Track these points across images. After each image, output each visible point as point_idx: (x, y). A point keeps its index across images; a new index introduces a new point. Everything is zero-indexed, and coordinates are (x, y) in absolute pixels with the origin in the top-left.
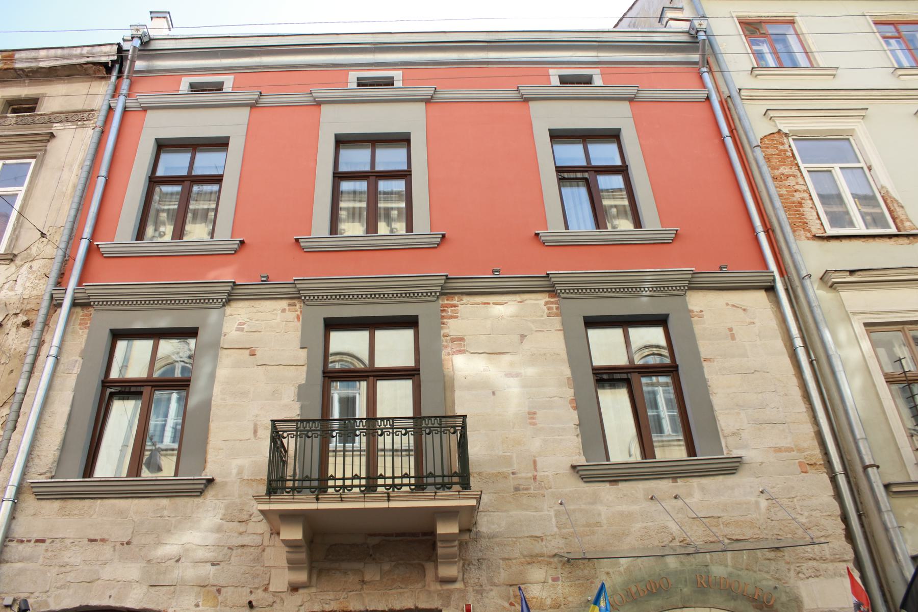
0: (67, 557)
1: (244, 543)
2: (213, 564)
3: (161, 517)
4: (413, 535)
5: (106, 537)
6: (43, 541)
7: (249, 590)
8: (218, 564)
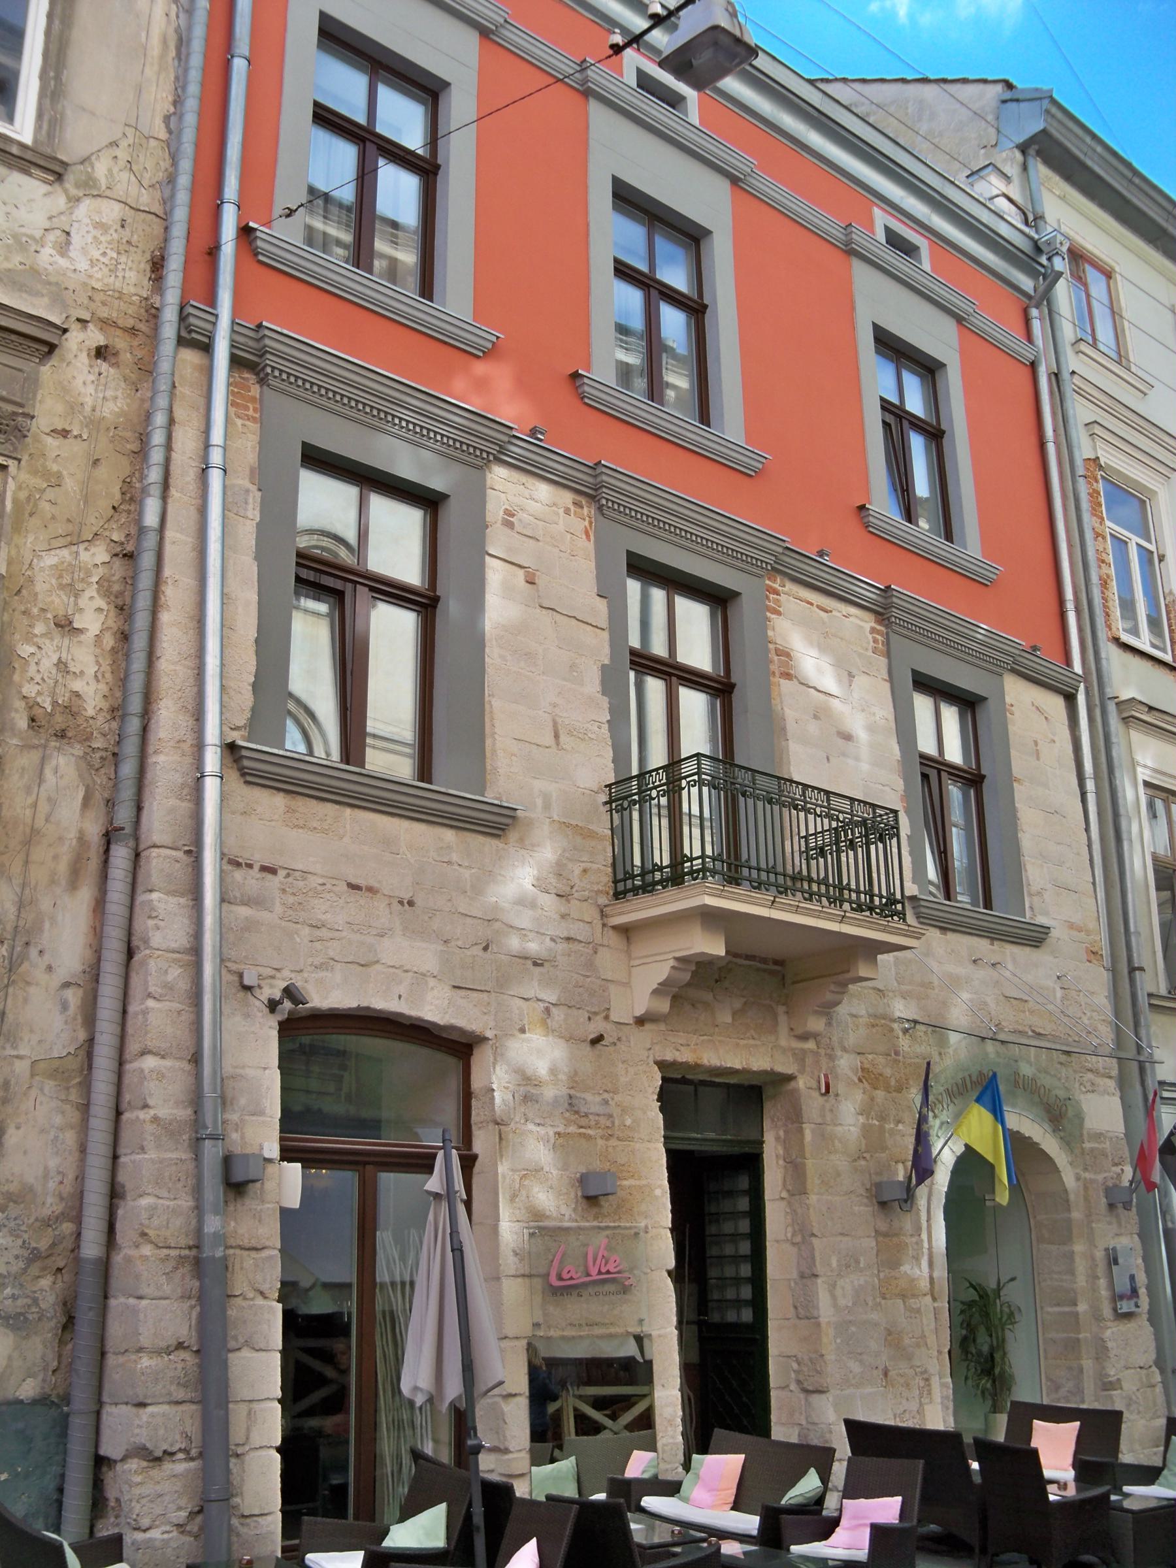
0: (320, 909)
2: (535, 964)
3: (449, 863)
4: (764, 960)
5: (376, 885)
6: (272, 871)
8: (542, 965)
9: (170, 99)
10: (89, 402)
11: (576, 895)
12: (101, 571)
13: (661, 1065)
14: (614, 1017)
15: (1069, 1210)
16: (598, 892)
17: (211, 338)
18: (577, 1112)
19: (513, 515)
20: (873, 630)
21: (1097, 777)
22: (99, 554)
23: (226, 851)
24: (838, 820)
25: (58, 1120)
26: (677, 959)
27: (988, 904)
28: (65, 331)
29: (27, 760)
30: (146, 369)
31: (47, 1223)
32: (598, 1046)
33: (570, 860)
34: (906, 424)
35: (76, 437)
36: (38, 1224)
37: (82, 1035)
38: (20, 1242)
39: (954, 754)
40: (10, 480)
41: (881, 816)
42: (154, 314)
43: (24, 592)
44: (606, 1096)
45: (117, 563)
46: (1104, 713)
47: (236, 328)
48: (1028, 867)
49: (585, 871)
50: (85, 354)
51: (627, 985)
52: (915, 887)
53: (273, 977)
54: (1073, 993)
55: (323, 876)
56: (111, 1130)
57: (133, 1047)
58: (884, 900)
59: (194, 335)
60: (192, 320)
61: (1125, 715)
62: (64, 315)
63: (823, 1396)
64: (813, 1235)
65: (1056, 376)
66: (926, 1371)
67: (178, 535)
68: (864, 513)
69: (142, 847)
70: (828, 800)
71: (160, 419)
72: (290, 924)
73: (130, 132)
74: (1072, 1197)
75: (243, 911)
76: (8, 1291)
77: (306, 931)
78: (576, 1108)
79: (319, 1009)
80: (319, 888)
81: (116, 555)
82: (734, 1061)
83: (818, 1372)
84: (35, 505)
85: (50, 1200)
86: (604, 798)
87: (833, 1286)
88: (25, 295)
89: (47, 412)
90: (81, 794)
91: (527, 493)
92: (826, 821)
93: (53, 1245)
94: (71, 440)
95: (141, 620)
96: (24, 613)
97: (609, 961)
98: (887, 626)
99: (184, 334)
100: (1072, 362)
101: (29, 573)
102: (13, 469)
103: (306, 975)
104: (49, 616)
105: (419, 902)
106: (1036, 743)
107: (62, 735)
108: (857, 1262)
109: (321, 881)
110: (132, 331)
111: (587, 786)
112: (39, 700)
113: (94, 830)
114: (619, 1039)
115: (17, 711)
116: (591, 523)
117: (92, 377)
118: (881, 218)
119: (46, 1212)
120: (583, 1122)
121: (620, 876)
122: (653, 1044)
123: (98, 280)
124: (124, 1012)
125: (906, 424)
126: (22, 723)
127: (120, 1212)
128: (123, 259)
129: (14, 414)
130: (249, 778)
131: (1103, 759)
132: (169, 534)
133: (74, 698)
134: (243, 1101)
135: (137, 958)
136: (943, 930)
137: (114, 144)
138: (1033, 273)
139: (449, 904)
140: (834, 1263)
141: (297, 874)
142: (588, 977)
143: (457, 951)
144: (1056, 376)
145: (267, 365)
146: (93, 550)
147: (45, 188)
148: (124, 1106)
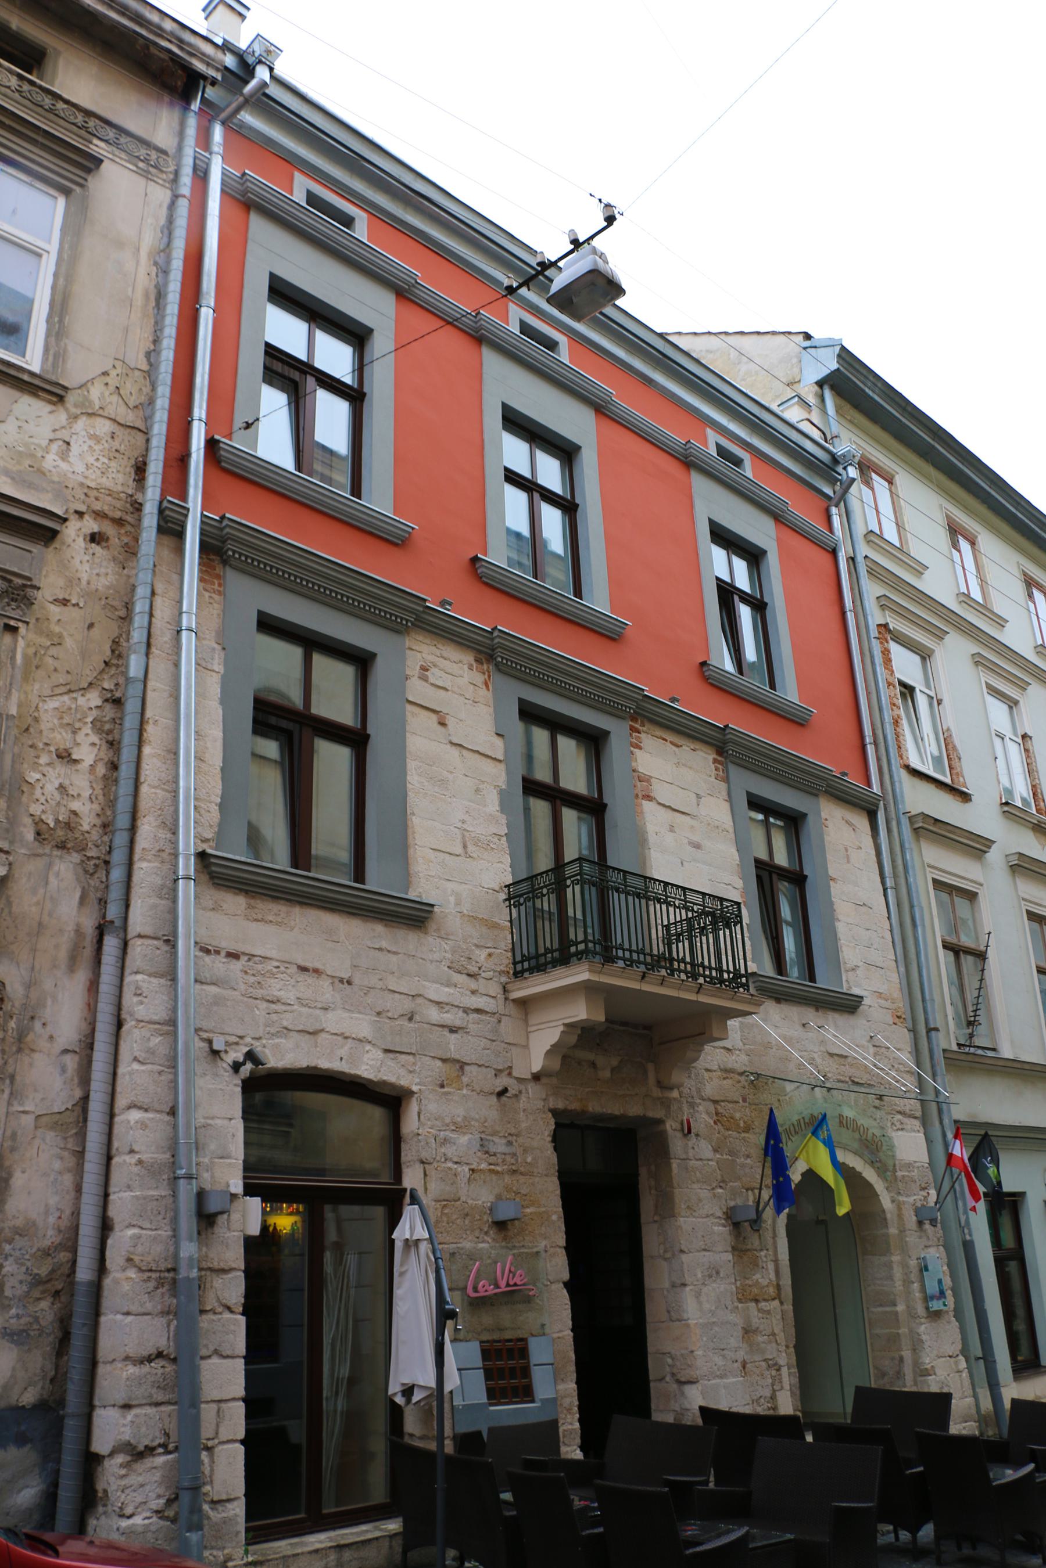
0: (275, 988)
1: (480, 1006)
3: (380, 949)
6: (233, 956)
7: (493, 1072)
9: (151, 339)
10: (85, 577)
11: (483, 974)
12: (95, 713)
13: (555, 1112)
14: (515, 1074)
15: (886, 1227)
16: (501, 972)
17: (183, 526)
18: (487, 1152)
19: (427, 670)
20: (715, 761)
21: (895, 876)
22: (94, 699)
23: (198, 940)
24: (693, 911)
25: (57, 1165)
26: (565, 1025)
27: (812, 979)
28: (65, 520)
29: (35, 866)
30: (131, 551)
31: (46, 1253)
32: (504, 1099)
33: (477, 946)
34: (736, 598)
35: (74, 605)
36: (40, 1253)
37: (78, 1093)
38: (24, 1269)
39: (781, 859)
40: (20, 639)
41: (727, 907)
42: (138, 507)
43: (31, 730)
44: (510, 1138)
45: (108, 706)
46: (899, 824)
47: (204, 519)
48: (844, 949)
49: (490, 955)
50: (81, 539)
51: (526, 1047)
52: (755, 965)
53: (237, 1044)
54: (883, 1050)
55: (277, 961)
56: (103, 1172)
57: (121, 1102)
58: (731, 975)
59: (170, 525)
60: (167, 512)
61: (917, 826)
62: (65, 508)
63: (694, 1386)
64: (682, 1251)
65: (852, 559)
66: (776, 1364)
67: (158, 685)
68: (705, 669)
69: (129, 937)
70: (685, 895)
71: (142, 591)
72: (251, 1000)
73: (118, 364)
74: (889, 1216)
75: (213, 989)
76: (13, 1311)
77: (265, 1005)
78: (486, 1149)
79: (276, 1069)
80: (275, 970)
81: (107, 700)
82: (614, 1108)
83: (689, 1366)
84: (41, 659)
85: (50, 1233)
86: (503, 896)
87: (698, 1295)
88: (33, 491)
89: (50, 585)
90: (78, 894)
91: (438, 652)
92: (683, 912)
93: (53, 1271)
94: (69, 609)
95: (127, 754)
96: (31, 746)
97: (509, 1028)
98: (726, 758)
99: (162, 523)
100: (863, 550)
101: (36, 714)
102: (23, 629)
103: (264, 1041)
104: (52, 749)
105: (356, 981)
106: (847, 850)
107: (62, 846)
108: (718, 1273)
109: (277, 964)
110: (119, 522)
111: (491, 886)
112: (43, 817)
113: (89, 925)
114: (520, 1092)
115: (25, 826)
116: (489, 676)
117: (87, 558)
118: (713, 437)
119: (47, 1243)
120: (492, 1159)
121: (518, 958)
122: (547, 1095)
123: (92, 480)
124: (115, 1074)
125: (736, 598)
126: (30, 836)
127: (110, 1242)
128: (113, 464)
129: (25, 586)
130: (216, 881)
131: (899, 861)
132: (151, 684)
133: (72, 816)
134: (212, 1147)
135: (125, 1028)
136: (778, 1001)
137: (105, 374)
138: (833, 481)
139: (381, 983)
140: (700, 1275)
141: (256, 959)
142: (494, 1041)
143: (387, 1021)
144: (852, 559)
145: (229, 549)
146: (88, 695)
147: (49, 407)
148: (114, 1151)
